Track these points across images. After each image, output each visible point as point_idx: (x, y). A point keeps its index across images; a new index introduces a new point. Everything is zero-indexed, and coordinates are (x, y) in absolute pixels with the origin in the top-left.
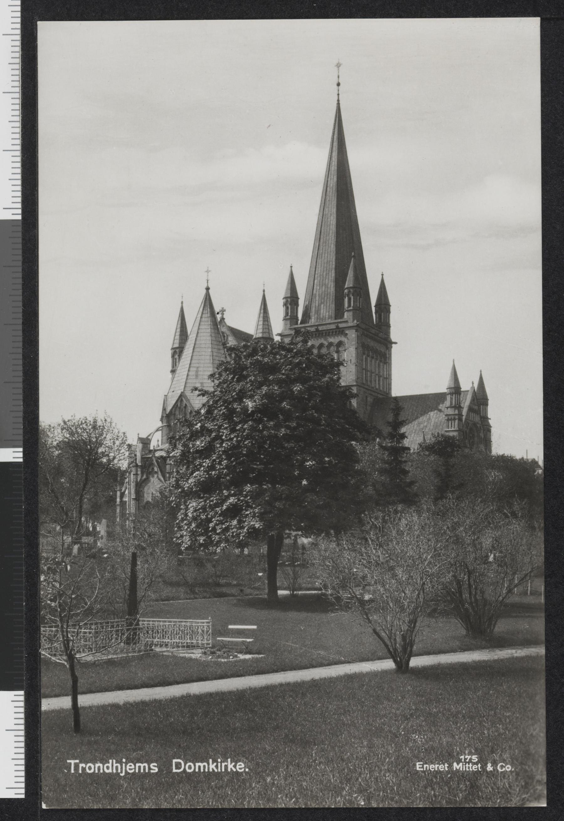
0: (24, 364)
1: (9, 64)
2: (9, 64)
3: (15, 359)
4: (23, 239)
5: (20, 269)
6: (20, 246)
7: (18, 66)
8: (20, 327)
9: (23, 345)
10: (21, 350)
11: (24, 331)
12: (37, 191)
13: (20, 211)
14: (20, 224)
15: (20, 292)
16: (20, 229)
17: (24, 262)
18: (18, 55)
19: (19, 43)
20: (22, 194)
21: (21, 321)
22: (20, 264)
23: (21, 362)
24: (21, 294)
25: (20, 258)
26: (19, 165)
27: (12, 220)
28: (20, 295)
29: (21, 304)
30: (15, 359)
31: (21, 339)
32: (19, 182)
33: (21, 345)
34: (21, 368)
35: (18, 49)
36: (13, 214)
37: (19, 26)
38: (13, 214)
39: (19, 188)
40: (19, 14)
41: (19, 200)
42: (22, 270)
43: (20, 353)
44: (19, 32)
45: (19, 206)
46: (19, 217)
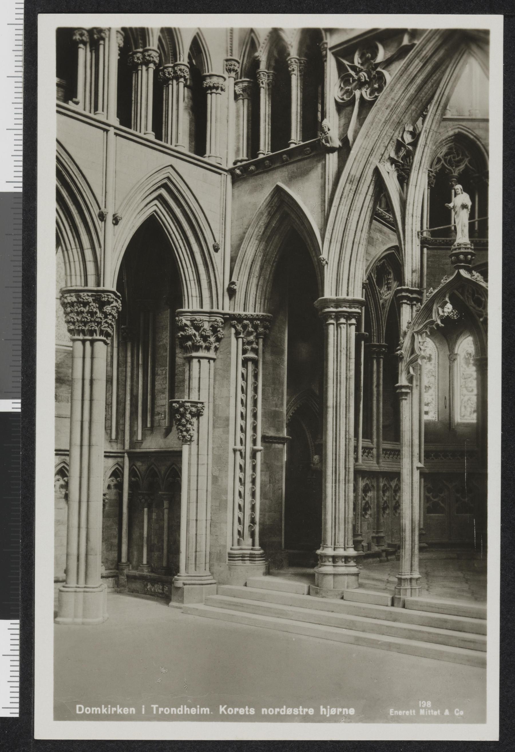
0: (23, 323)
1: (13, 51)
2: (13, 51)
4: (23, 210)
5: (21, 237)
6: (21, 216)
7: (22, 53)
9: (23, 306)
10: (20, 311)
11: (23, 292)
12: (36, 166)
13: (21, 185)
14: (22, 196)
15: (20, 258)
16: (21, 200)
17: (24, 231)
18: (22, 43)
19: (22, 32)
21: (20, 285)
22: (21, 232)
23: (20, 321)
24: (21, 259)
25: (21, 227)
29: (20, 269)
30: (15, 319)
31: (20, 300)
32: (21, 158)
33: (20, 305)
34: (20, 327)
35: (22, 37)
36: (15, 187)
37: (22, 16)
38: (15, 187)
39: (21, 164)
41: (21, 174)
42: (23, 238)
44: (22, 22)
45: (21, 179)
46: (21, 190)
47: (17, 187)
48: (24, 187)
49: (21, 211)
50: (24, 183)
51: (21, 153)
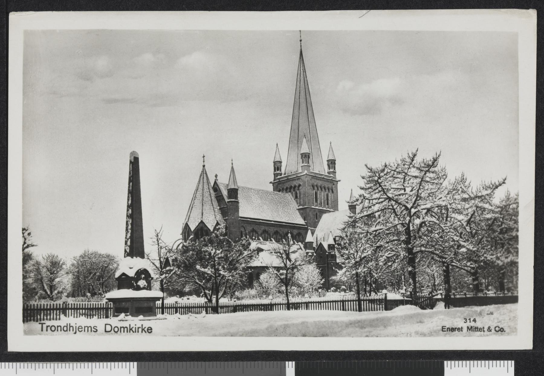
1: (35, 370)
2: (35, 370)
3: (228, 366)
4: (150, 361)
5: (169, 363)
6: (154, 363)
7: (37, 364)
8: (207, 363)
10: (222, 363)
11: (209, 361)
12: (118, 352)
13: (132, 363)
16: (143, 363)
17: (165, 361)
18: (30, 364)
19: (22, 364)
20: (121, 362)
21: (203, 363)
22: (166, 363)
23: (230, 363)
24: (185, 362)
25: (162, 363)
27: (137, 368)
28: (186, 363)
29: (192, 363)
30: (228, 366)
31: (215, 363)
33: (218, 363)
35: (26, 364)
36: (133, 368)
37: (11, 364)
38: (133, 368)
43: (224, 363)
46: (136, 363)
47: (133, 366)
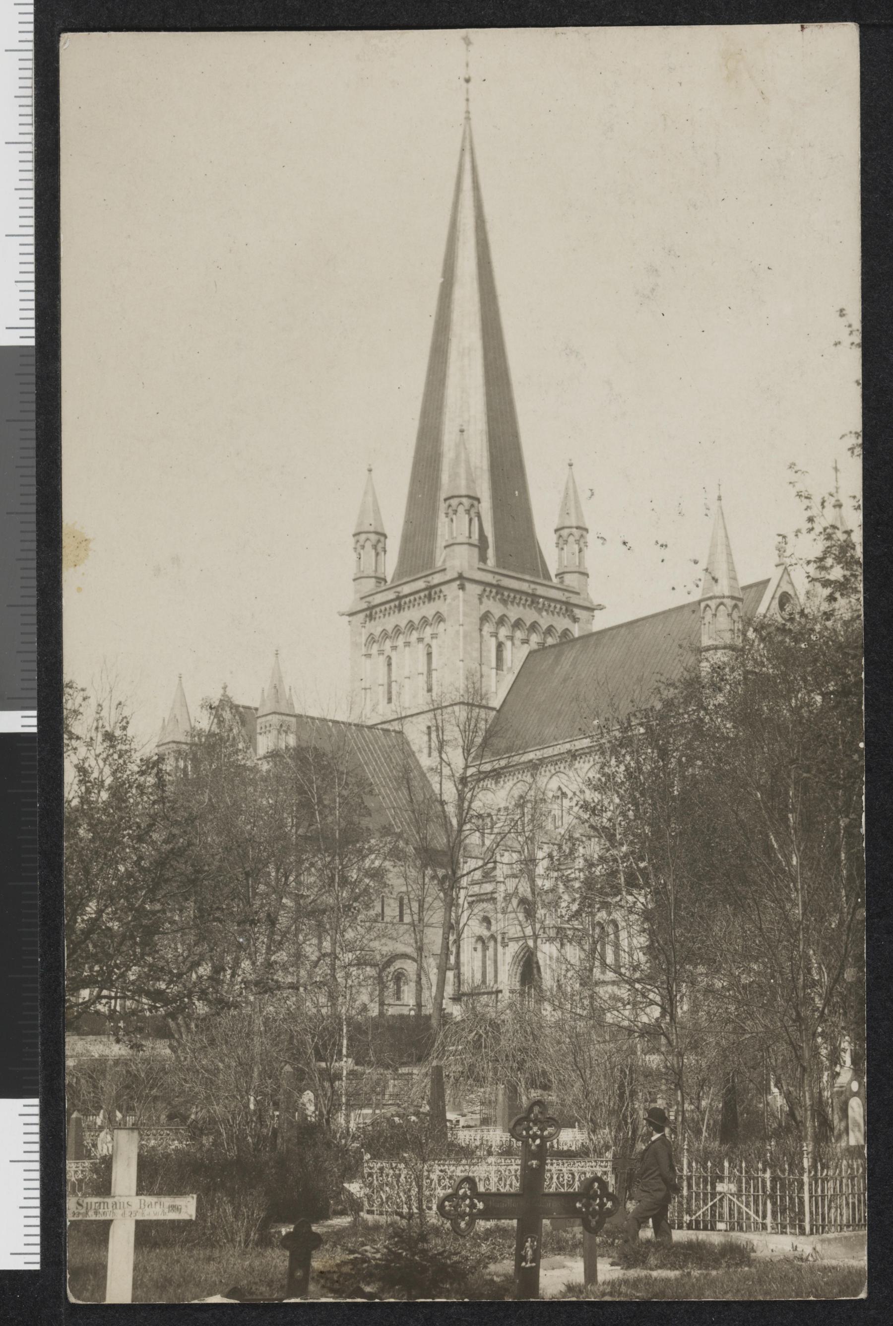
4: (38, 377)
5: (33, 425)
6: (33, 388)
7: (31, 101)
8: (34, 518)
9: (38, 547)
10: (33, 555)
12: (59, 299)
13: (32, 333)
14: (33, 352)
16: (33, 360)
17: (38, 414)
18: (30, 83)
19: (31, 64)
21: (34, 508)
22: (33, 416)
23: (34, 573)
26: (32, 258)
29: (34, 481)
31: (34, 536)
32: (32, 286)
33: (34, 545)
34: (34, 583)
35: (30, 73)
37: (31, 37)
39: (32, 295)
40: (31, 18)
41: (32, 314)
44: (31, 46)
45: (32, 323)
46: (32, 342)
47: (25, 337)
48: (38, 337)
49: (33, 379)
50: (38, 329)
51: (32, 277)
